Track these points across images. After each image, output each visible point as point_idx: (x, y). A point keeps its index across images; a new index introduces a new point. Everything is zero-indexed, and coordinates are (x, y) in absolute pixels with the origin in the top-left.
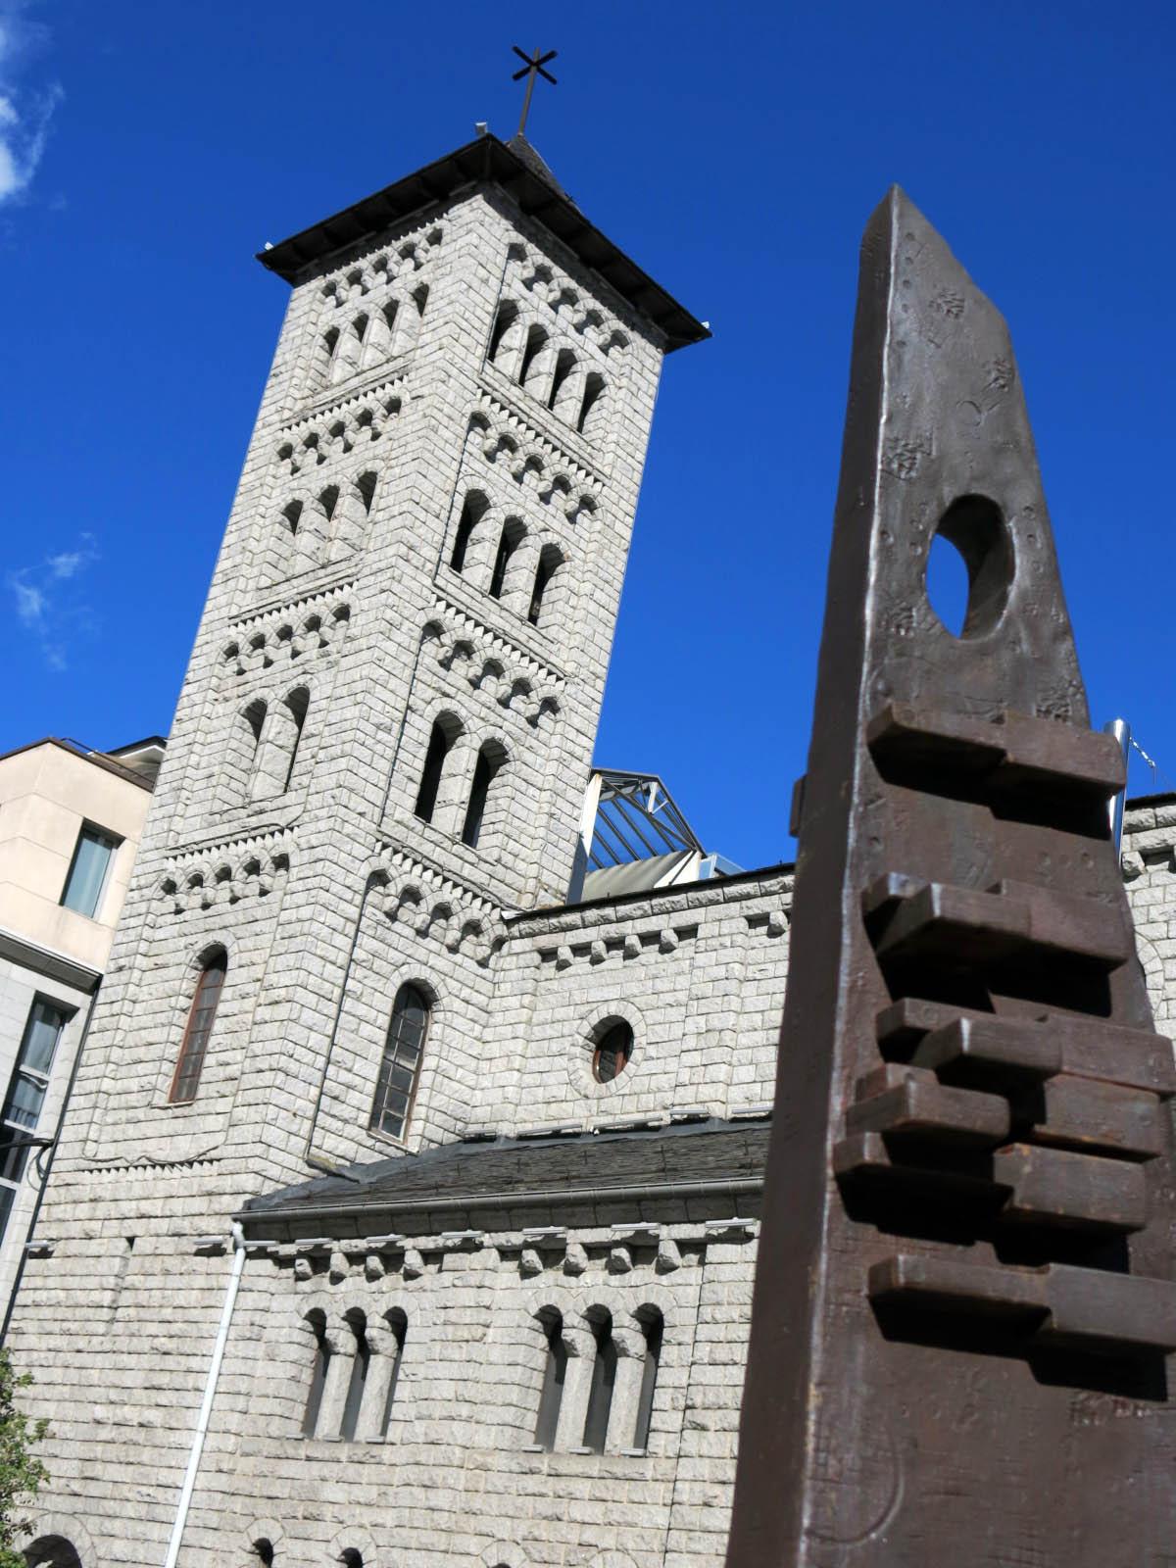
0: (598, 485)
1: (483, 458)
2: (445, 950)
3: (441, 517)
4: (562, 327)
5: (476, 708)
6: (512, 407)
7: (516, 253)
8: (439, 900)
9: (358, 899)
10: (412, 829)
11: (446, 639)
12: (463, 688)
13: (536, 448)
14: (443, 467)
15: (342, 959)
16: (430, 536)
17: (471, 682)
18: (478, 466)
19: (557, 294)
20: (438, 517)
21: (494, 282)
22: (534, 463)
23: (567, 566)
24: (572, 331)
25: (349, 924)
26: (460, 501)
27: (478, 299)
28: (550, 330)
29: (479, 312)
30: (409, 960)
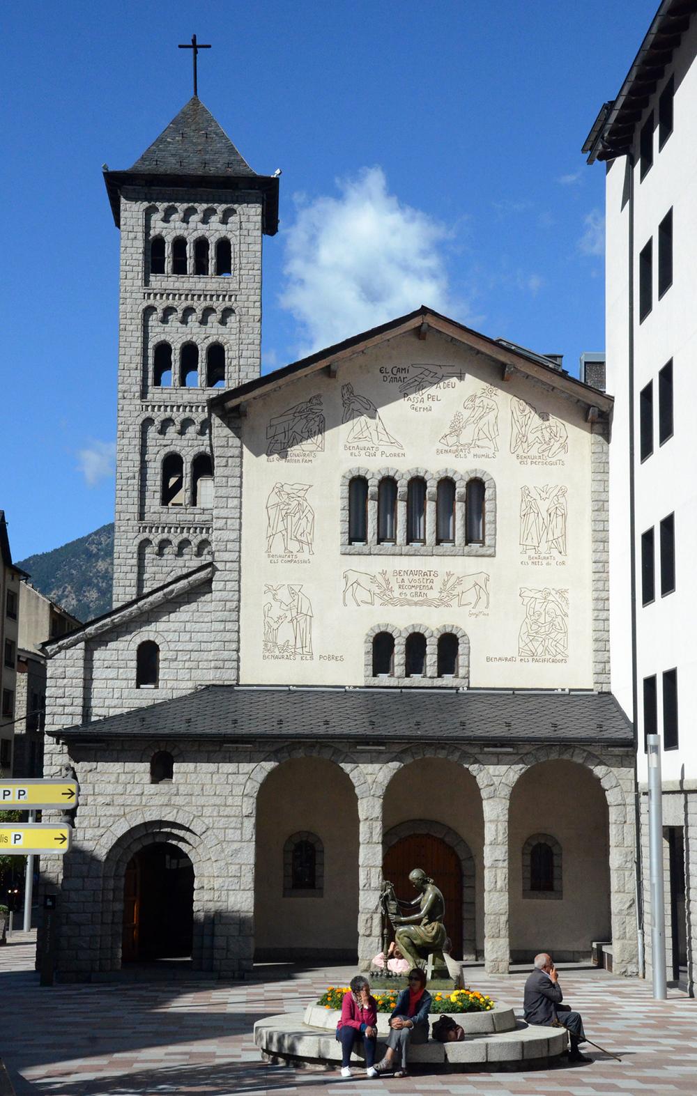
0: (233, 298)
1: (160, 324)
2: (194, 557)
3: (139, 368)
4: (193, 230)
5: (185, 443)
6: (167, 292)
7: (149, 213)
8: (181, 539)
9: (135, 555)
10: (162, 513)
11: (156, 423)
12: (175, 438)
13: (189, 303)
14: (133, 345)
15: (134, 582)
16: (134, 381)
17: (179, 434)
18: (158, 330)
19: (182, 215)
20: (136, 369)
21: (140, 236)
22: (189, 311)
23: (226, 349)
24: (200, 225)
25: (133, 567)
26: (151, 353)
27: (133, 250)
28: (185, 234)
29: (135, 256)
30: (174, 569)
